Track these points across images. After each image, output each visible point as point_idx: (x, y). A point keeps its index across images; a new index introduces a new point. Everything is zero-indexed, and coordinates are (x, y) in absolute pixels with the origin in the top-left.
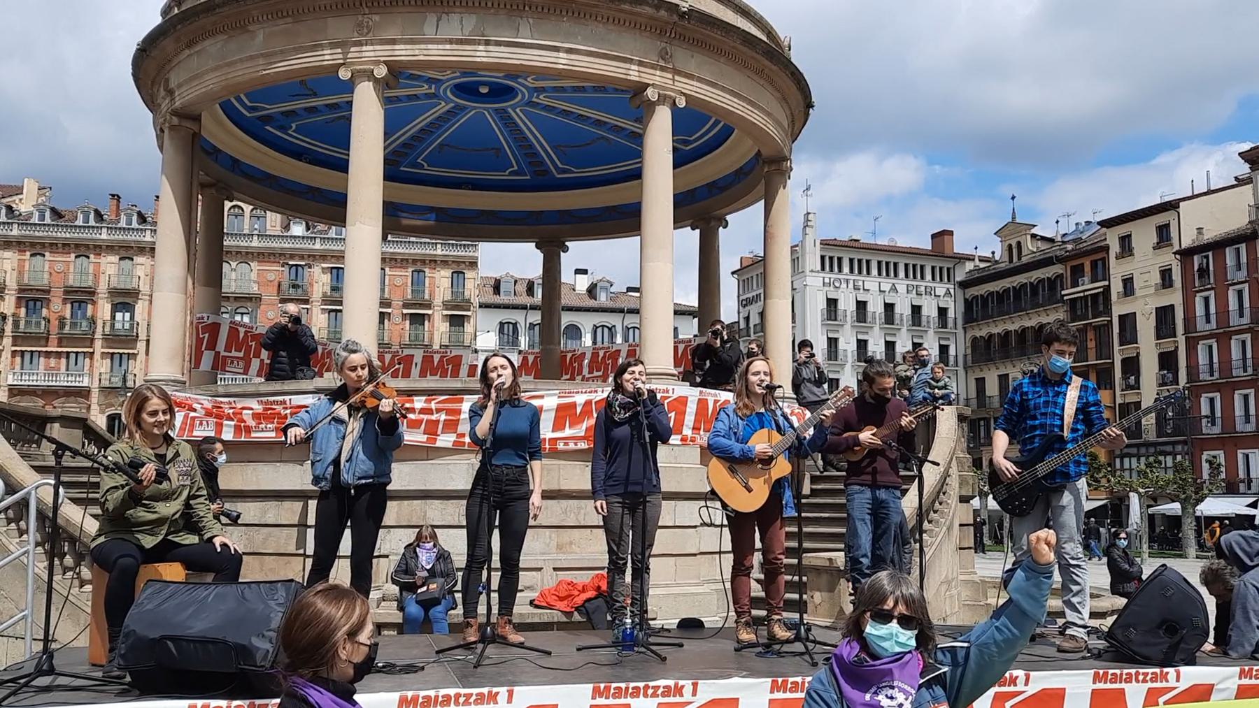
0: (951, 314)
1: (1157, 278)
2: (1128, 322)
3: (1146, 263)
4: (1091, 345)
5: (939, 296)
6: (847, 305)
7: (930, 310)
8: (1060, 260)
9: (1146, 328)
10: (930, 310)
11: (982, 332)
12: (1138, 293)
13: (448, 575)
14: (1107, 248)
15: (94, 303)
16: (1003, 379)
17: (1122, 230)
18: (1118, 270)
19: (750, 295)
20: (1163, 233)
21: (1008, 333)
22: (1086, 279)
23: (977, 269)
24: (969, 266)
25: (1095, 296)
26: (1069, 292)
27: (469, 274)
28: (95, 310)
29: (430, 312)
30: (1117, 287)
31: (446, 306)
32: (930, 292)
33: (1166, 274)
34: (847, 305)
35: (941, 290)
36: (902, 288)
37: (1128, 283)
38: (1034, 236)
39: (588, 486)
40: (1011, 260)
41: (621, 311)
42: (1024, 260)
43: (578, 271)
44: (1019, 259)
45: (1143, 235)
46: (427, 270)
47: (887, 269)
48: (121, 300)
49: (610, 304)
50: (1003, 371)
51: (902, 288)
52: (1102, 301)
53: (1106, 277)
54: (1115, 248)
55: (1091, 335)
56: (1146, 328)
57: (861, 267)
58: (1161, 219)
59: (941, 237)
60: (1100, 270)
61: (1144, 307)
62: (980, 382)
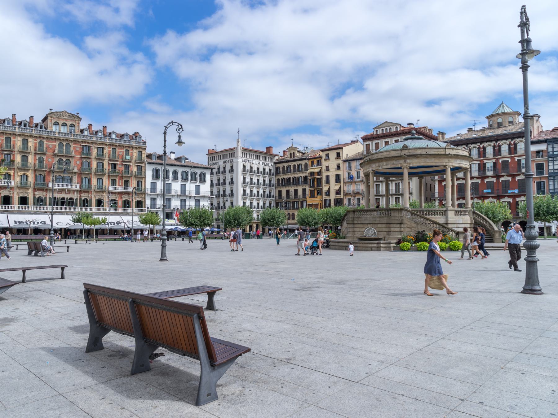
0: (272, 172)
1: (336, 167)
2: (328, 177)
3: (333, 162)
4: (316, 183)
5: (269, 166)
6: (248, 167)
7: (267, 170)
8: (309, 159)
9: (332, 180)
10: (267, 170)
11: (281, 177)
12: (330, 170)
13: (401, 224)
14: (321, 157)
15: (14, 155)
16: (288, 192)
17: (327, 152)
18: (325, 163)
19: (214, 162)
20: (338, 155)
21: (290, 178)
23: (279, 159)
24: (277, 158)
27: (143, 152)
28: (14, 157)
31: (136, 162)
32: (268, 165)
34: (248, 167)
35: (270, 165)
36: (261, 163)
38: (298, 151)
39: (449, 212)
40: (291, 157)
41: (190, 167)
42: (296, 158)
43: (171, 153)
44: (294, 157)
45: (333, 155)
46: (130, 150)
47: (258, 157)
49: (186, 164)
50: (287, 189)
51: (261, 163)
52: (320, 173)
53: (321, 165)
54: (324, 157)
55: (316, 180)
56: (332, 180)
57: (251, 156)
58: (338, 151)
59: (269, 149)
60: (319, 163)
61: (332, 174)
62: (280, 192)
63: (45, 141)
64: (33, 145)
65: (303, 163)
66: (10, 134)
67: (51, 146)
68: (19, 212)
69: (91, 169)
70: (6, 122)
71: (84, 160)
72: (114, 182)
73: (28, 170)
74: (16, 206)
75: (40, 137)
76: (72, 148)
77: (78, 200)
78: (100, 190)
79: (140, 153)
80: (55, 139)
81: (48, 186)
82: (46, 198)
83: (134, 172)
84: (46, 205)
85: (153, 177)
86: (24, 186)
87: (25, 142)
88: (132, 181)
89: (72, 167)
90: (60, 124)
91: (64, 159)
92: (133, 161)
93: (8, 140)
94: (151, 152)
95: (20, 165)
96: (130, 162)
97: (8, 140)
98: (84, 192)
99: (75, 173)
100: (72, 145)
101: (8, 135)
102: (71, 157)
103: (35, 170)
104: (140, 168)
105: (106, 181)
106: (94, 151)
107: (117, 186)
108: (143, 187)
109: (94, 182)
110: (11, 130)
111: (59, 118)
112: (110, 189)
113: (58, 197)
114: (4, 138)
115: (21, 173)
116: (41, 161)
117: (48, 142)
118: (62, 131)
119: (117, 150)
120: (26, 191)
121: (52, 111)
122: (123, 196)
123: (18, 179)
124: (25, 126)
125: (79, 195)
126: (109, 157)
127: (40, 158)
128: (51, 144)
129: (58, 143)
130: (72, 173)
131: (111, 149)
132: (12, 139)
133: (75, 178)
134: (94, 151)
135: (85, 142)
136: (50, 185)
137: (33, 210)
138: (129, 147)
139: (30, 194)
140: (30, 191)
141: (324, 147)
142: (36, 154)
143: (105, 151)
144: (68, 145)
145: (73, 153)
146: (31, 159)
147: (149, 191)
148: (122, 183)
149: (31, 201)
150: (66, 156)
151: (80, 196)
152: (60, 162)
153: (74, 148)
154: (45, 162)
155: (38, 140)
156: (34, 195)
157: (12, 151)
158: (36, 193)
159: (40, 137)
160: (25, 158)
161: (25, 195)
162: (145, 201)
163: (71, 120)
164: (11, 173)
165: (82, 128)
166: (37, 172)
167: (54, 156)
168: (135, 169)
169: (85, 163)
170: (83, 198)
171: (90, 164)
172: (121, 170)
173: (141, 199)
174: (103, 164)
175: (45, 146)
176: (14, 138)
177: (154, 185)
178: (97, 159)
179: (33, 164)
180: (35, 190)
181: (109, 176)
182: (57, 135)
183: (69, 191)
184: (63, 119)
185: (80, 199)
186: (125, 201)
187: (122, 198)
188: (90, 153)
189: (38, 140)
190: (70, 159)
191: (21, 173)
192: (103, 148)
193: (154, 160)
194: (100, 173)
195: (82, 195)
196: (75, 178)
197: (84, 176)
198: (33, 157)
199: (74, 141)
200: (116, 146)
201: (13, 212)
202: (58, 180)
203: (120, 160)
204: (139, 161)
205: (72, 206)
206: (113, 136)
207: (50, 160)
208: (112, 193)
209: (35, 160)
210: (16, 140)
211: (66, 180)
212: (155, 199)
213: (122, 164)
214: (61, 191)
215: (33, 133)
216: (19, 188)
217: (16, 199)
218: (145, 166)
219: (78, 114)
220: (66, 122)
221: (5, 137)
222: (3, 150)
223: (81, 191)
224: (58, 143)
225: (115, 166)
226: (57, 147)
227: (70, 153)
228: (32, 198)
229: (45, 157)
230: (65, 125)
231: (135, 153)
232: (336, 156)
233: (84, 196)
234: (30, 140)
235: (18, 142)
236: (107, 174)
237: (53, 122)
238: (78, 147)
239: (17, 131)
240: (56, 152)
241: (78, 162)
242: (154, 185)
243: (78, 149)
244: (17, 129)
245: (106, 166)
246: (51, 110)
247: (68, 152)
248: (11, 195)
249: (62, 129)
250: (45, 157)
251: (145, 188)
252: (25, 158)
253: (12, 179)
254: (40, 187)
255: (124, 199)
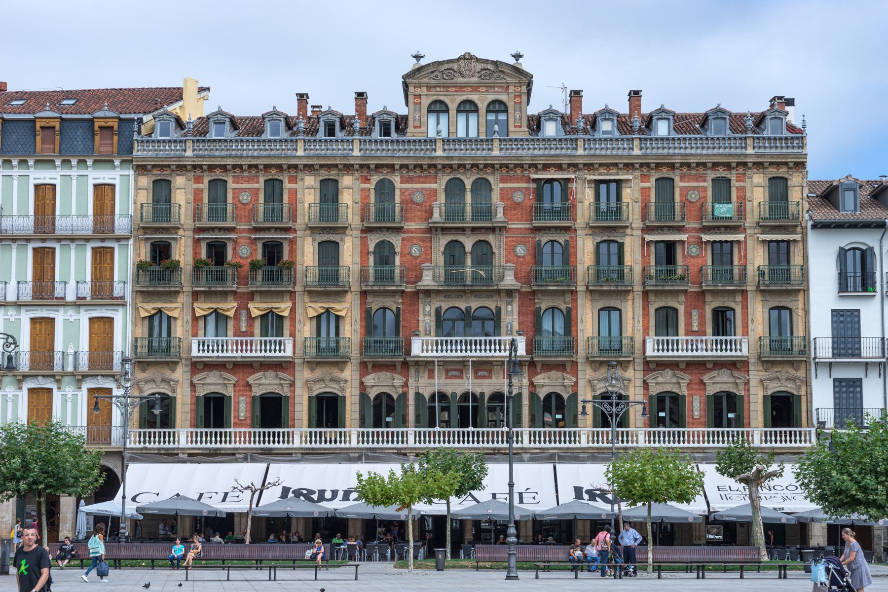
15: (293, 242)
27: (795, 180)
29: (741, 237)
46: (733, 176)
48: (325, 238)
63: (396, 179)
64: (358, 197)
66: (279, 167)
67: (418, 198)
68: (194, 457)
69: (570, 274)
70: (268, 126)
71: (544, 238)
72: (666, 322)
73: (340, 294)
74: (299, 435)
75: (378, 167)
76: (496, 197)
77: (526, 401)
78: (611, 356)
79: (778, 188)
80: (432, 168)
81: (408, 352)
82: (404, 396)
83: (751, 271)
84: (404, 423)
85: (843, 286)
86: (327, 357)
87: (329, 191)
88: (745, 308)
89: (496, 271)
90: (453, 107)
91: (468, 242)
92: (750, 221)
93: (273, 188)
94: (834, 175)
95: (313, 276)
96: (736, 229)
97: (273, 188)
98: (548, 367)
99: (510, 293)
100: (497, 185)
101: (273, 174)
102: (493, 230)
103: (364, 294)
104: (780, 253)
105: (634, 317)
106: (585, 198)
107: (682, 337)
108: (799, 331)
109: (587, 323)
110: (280, 153)
111: (446, 87)
112: (649, 352)
113: (478, 391)
114: (261, 185)
115: (315, 308)
116: (384, 255)
117: (410, 180)
118: (461, 134)
119: (679, 184)
120: (336, 373)
121: (423, 62)
122: (706, 378)
123: (306, 330)
124: (331, 131)
125: (525, 381)
126: (644, 217)
127: (380, 245)
128: (418, 187)
129: (444, 179)
130: (498, 292)
131: (651, 184)
132: (287, 185)
133: (511, 315)
134: (585, 198)
135: (546, 167)
136: (417, 349)
137: (354, 444)
138: (728, 166)
139: (349, 384)
140: (350, 373)
142: (367, 230)
143: (628, 194)
144: (482, 187)
145: (500, 216)
146: (349, 252)
147: (824, 349)
148: (702, 320)
149: (351, 410)
150: (474, 229)
151: (532, 385)
152: (454, 254)
153: (504, 194)
154: (398, 260)
155: (375, 179)
156: (362, 385)
157: (287, 230)
158: (369, 380)
159: (378, 167)
160: (329, 253)
161: (333, 388)
162: (809, 395)
163: (490, 87)
164: (284, 307)
165: (534, 109)
166: (370, 299)
167: (433, 230)
168: (758, 258)
169: (547, 249)
170: (542, 393)
171: (568, 251)
172: (697, 262)
173: (790, 387)
174: (621, 246)
175: (397, 199)
176: (293, 180)
177: (846, 325)
178: (594, 230)
179: (356, 269)
180: (365, 367)
181: (646, 294)
182: (439, 153)
183: (484, 367)
184: (461, 88)
185: (533, 396)
186: (717, 399)
187: (703, 384)
188: (567, 210)
189: (375, 179)
190: (491, 238)
191: (315, 308)
192: (618, 182)
193: (848, 210)
194: (610, 284)
195: (539, 379)
196: (511, 315)
197: (544, 304)
198: (358, 242)
199: (504, 168)
200: (672, 166)
201: (287, 456)
202: (447, 325)
203: (692, 225)
204: (779, 217)
205: (432, 424)
206: (662, 129)
207: (415, 251)
208: (661, 365)
209: (364, 253)
210: (298, 186)
211: (476, 324)
212: (856, 384)
213: (700, 242)
214: (455, 368)
215: (356, 153)
216: (312, 364)
217: (301, 409)
218: (804, 241)
219: (517, 57)
220: (474, 97)
221: (262, 180)
222: (257, 230)
223: (532, 364)
224: (444, 179)
225: (669, 250)
226: (442, 198)
227: (489, 214)
228: (356, 399)
229: (397, 241)
230: (468, 107)
231: (756, 191)
233: (547, 383)
234: (347, 180)
235: (306, 193)
236: (638, 288)
237: (426, 102)
238: (521, 190)
239: (300, 152)
240: (436, 217)
241: (520, 250)
242: (846, 325)
243: (518, 197)
244: (300, 144)
245: (634, 257)
246: (418, 57)
247: (484, 211)
248: (285, 392)
249: (467, 127)
250: (397, 241)
251: (806, 338)
252: (329, 253)
253: (286, 332)
254: (383, 356)
255: (711, 390)
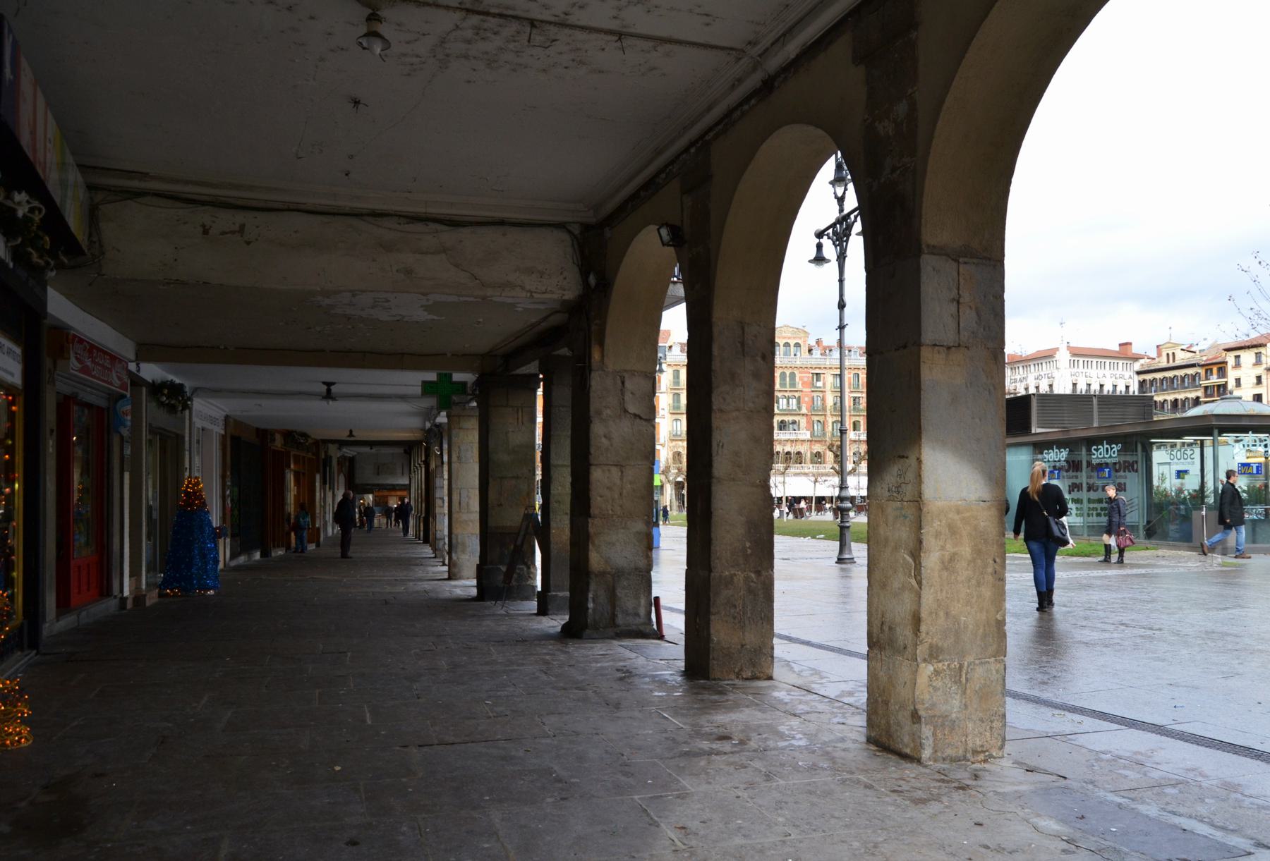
14: (1226, 363)
17: (1237, 353)
22: (1215, 376)
25: (1219, 386)
26: (1204, 383)
30: (1231, 385)
32: (1122, 377)
33: (1259, 379)
36: (1108, 375)
37: (1238, 381)
42: (1178, 363)
51: (1108, 375)
60: (1222, 371)
65: (1191, 371)
69: (824, 409)
141: (1231, 341)
171: (823, 399)
232: (1253, 360)
